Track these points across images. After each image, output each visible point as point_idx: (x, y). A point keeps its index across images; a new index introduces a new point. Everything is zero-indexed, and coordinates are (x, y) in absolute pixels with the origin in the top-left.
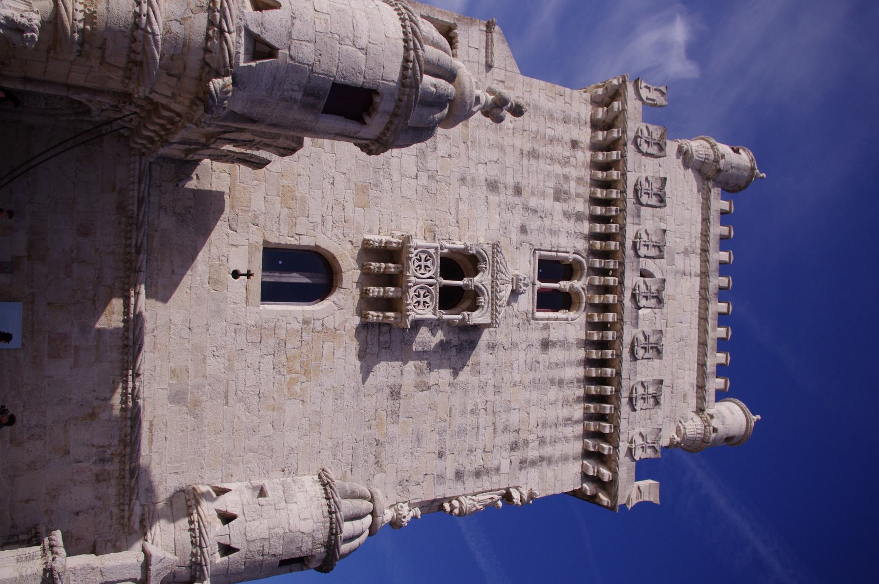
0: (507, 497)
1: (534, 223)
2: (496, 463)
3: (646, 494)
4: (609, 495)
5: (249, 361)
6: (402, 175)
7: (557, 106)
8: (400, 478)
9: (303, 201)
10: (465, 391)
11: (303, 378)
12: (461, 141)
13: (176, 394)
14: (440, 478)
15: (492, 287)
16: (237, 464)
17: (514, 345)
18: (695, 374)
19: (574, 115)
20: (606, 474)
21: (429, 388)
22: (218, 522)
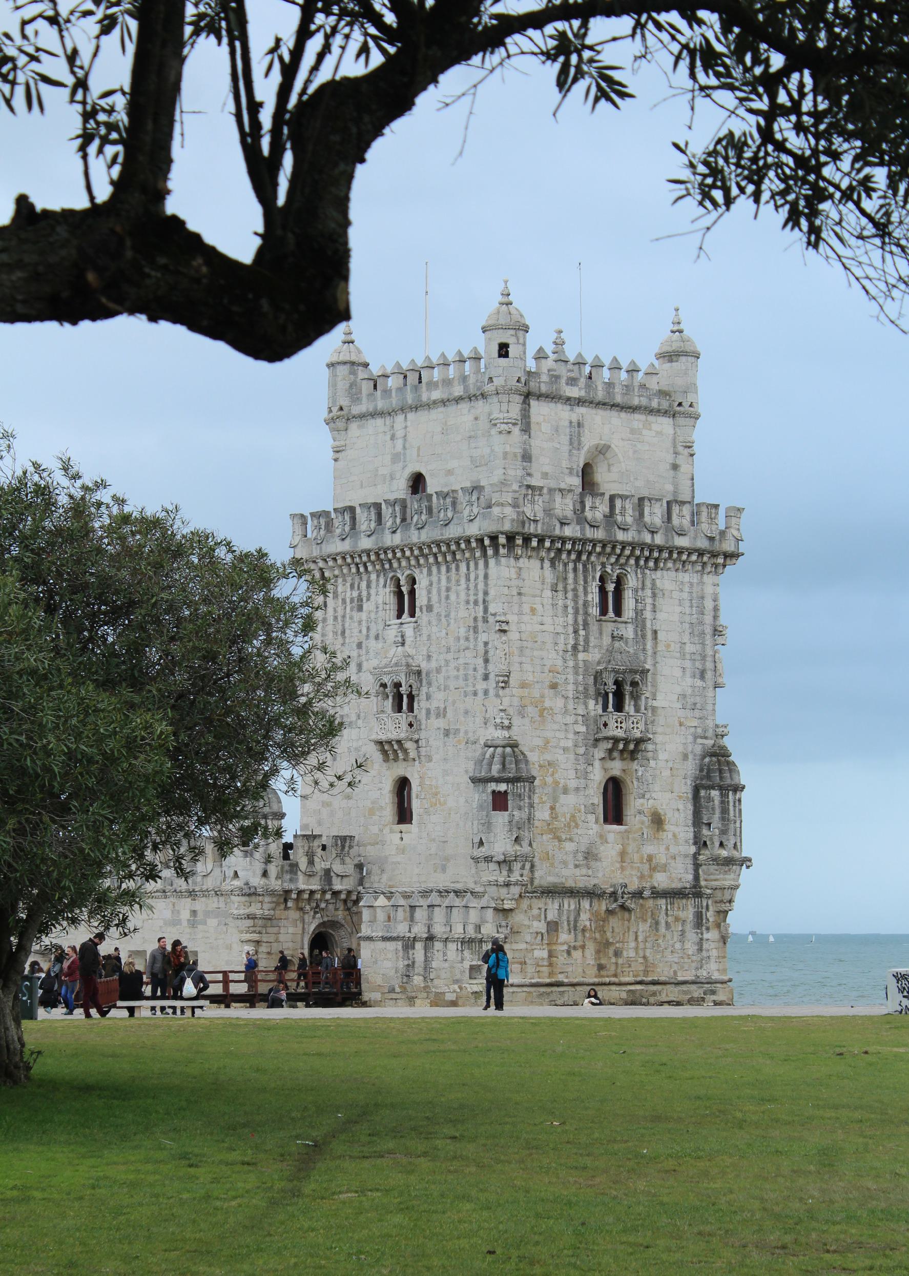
9: (373, 803)
14: (486, 692)
20: (487, 542)
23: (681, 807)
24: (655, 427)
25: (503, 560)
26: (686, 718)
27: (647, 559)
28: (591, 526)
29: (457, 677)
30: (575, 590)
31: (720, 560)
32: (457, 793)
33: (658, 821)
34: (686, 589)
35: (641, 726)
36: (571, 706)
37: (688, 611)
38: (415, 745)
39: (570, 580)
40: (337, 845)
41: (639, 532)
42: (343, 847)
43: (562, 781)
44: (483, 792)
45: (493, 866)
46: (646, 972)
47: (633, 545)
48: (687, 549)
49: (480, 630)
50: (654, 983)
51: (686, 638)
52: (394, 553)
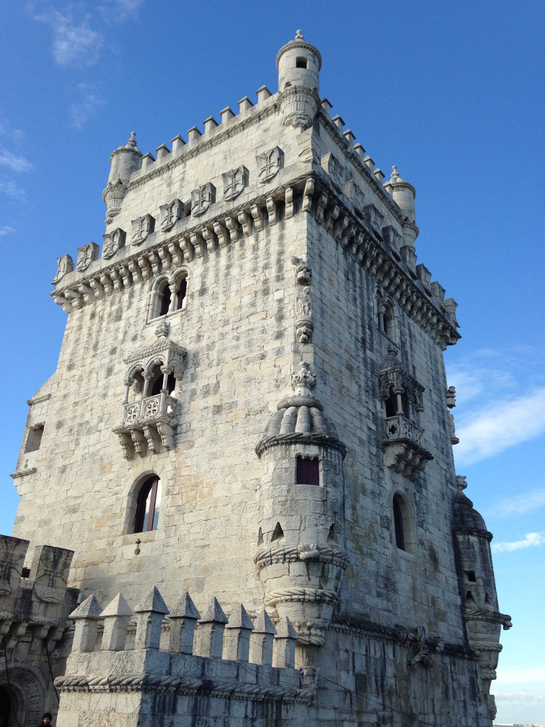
0: (303, 282)
1: (132, 332)
2: (275, 305)
3: (305, 145)
4: (304, 184)
5: (185, 532)
6: (99, 442)
7: (72, 337)
8: (274, 389)
9: (104, 511)
10: (224, 350)
11: (201, 486)
12: (85, 404)
13: (198, 587)
15: (149, 356)
16: (247, 530)
17: (200, 319)
18: (252, 127)
19: (78, 323)
20: (289, 194)
21: (218, 382)
22: (264, 544)
25: (305, 214)
29: (237, 347)
30: (361, 288)
32: (230, 477)
36: (364, 398)
38: (171, 432)
39: (358, 278)
40: (47, 559)
42: (55, 563)
43: (360, 477)
44: (283, 458)
45: (297, 568)
49: (272, 288)
52: (166, 250)
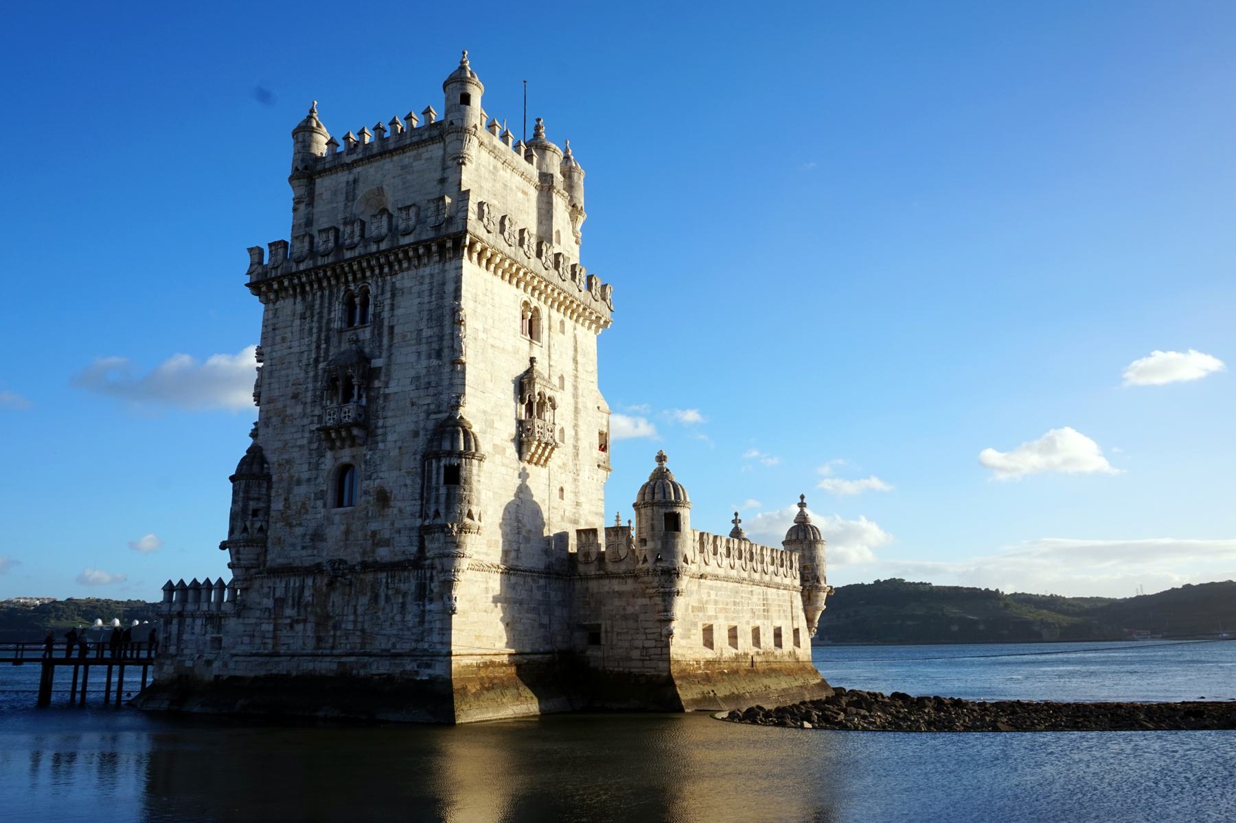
23: (409, 482)
24: (425, 156)
26: (419, 397)
27: (381, 267)
28: (323, 256)
30: (320, 313)
31: (449, 244)
33: (383, 498)
34: (427, 280)
35: (352, 414)
36: (309, 410)
37: (426, 299)
39: (317, 307)
41: (366, 247)
46: (363, 644)
47: (359, 259)
48: (409, 245)
50: (370, 655)
51: (423, 325)
